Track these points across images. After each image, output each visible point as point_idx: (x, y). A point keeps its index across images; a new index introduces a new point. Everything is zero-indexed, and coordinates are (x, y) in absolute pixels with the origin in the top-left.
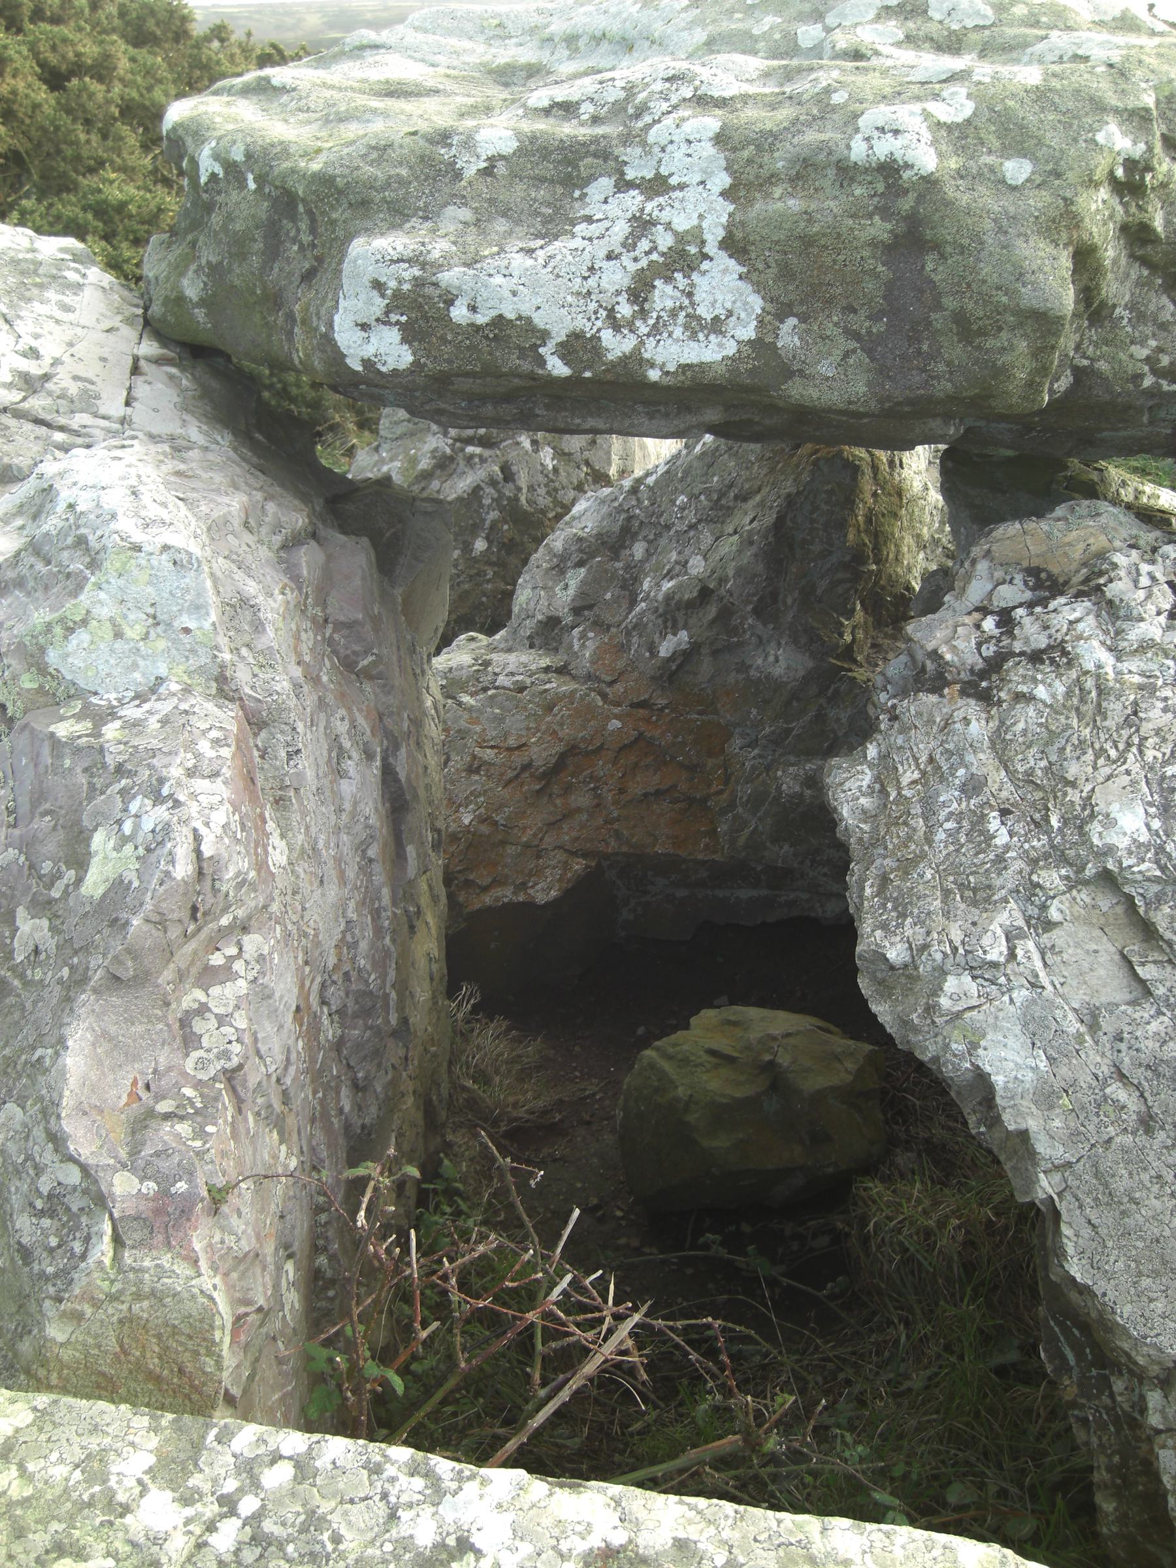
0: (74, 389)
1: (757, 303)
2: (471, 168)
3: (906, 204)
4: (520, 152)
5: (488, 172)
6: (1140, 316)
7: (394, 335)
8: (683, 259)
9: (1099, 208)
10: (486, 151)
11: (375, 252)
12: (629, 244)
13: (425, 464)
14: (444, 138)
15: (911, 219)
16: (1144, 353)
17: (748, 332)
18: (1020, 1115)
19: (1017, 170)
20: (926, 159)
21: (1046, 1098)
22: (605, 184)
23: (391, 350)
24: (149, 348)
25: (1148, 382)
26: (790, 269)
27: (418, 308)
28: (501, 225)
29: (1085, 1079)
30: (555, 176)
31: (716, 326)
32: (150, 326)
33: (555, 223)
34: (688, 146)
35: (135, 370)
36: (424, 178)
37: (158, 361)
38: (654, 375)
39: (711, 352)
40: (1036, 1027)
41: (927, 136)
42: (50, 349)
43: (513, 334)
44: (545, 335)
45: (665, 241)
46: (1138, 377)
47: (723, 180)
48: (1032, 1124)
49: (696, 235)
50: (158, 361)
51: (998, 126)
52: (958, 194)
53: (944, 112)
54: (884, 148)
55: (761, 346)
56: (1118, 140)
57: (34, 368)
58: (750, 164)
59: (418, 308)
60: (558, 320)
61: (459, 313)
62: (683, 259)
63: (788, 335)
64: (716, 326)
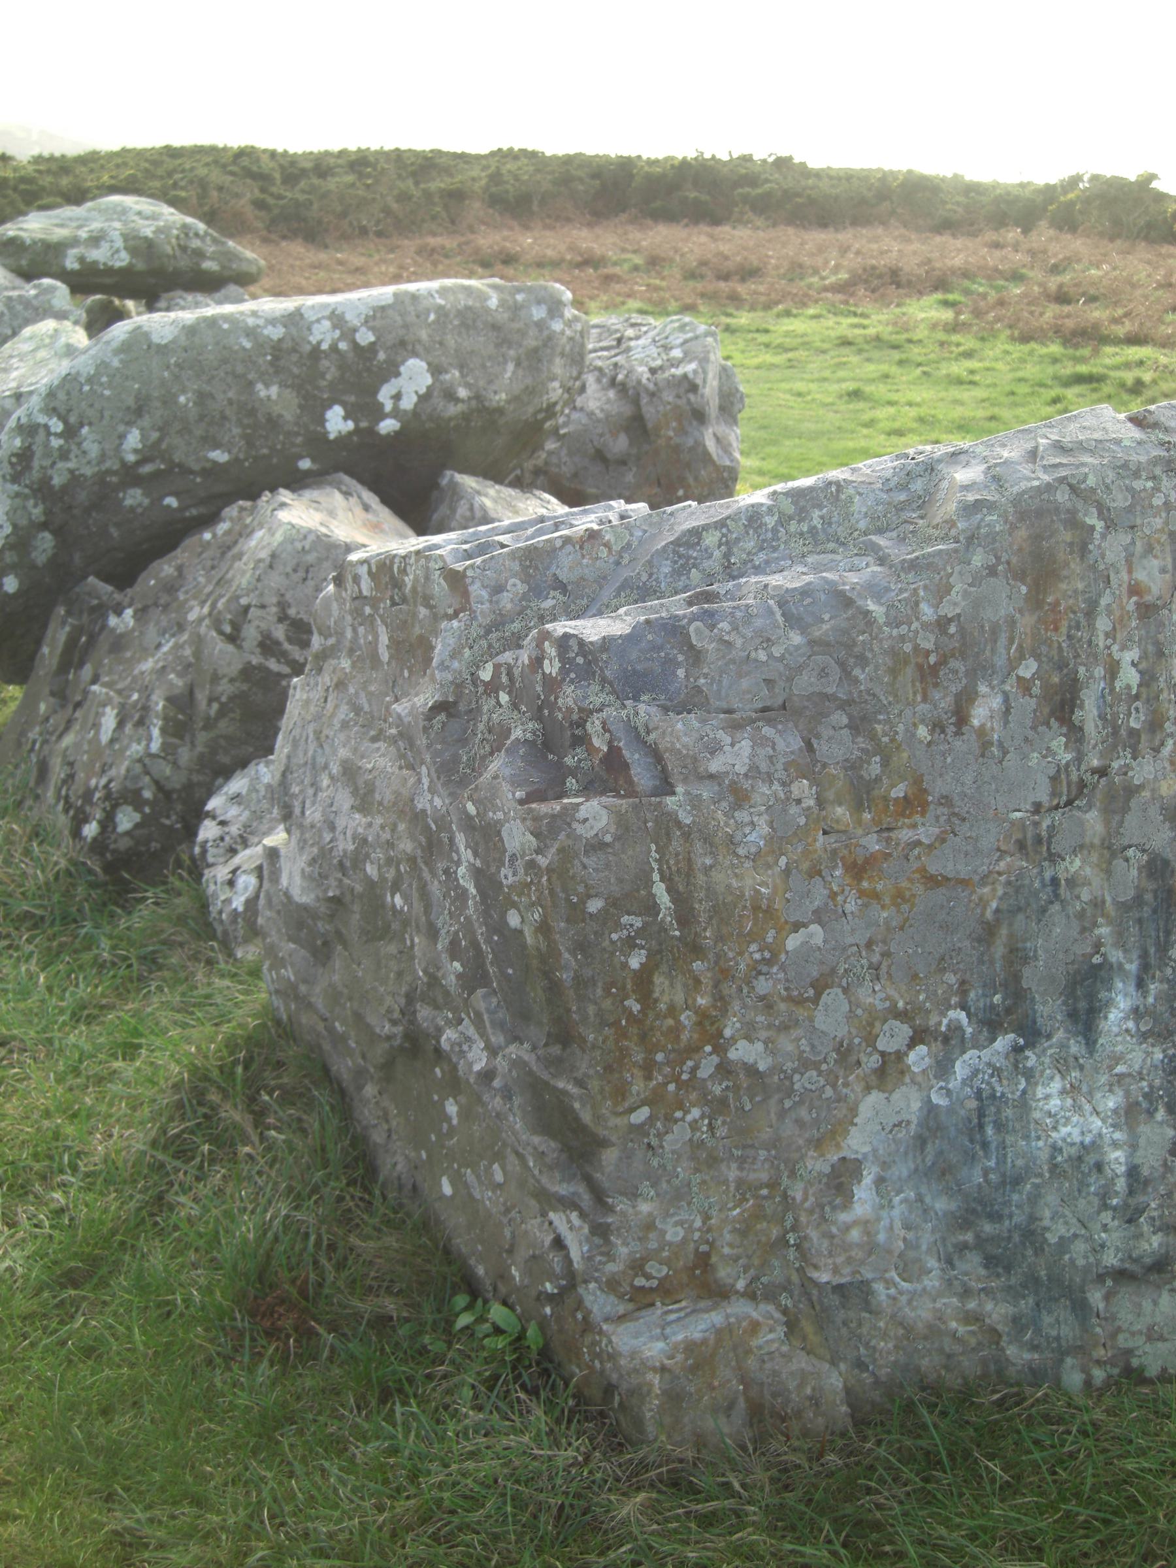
8: (117, 251)
9: (174, 241)
11: (73, 252)
15: (149, 244)
20: (151, 235)
23: (76, 266)
26: (133, 251)
27: (81, 260)
30: (95, 240)
34: (116, 235)
36: (75, 242)
39: (124, 264)
43: (95, 263)
51: (158, 231)
55: (130, 263)
56: (175, 232)
58: (126, 237)
59: (81, 260)
60: (102, 260)
62: (117, 251)
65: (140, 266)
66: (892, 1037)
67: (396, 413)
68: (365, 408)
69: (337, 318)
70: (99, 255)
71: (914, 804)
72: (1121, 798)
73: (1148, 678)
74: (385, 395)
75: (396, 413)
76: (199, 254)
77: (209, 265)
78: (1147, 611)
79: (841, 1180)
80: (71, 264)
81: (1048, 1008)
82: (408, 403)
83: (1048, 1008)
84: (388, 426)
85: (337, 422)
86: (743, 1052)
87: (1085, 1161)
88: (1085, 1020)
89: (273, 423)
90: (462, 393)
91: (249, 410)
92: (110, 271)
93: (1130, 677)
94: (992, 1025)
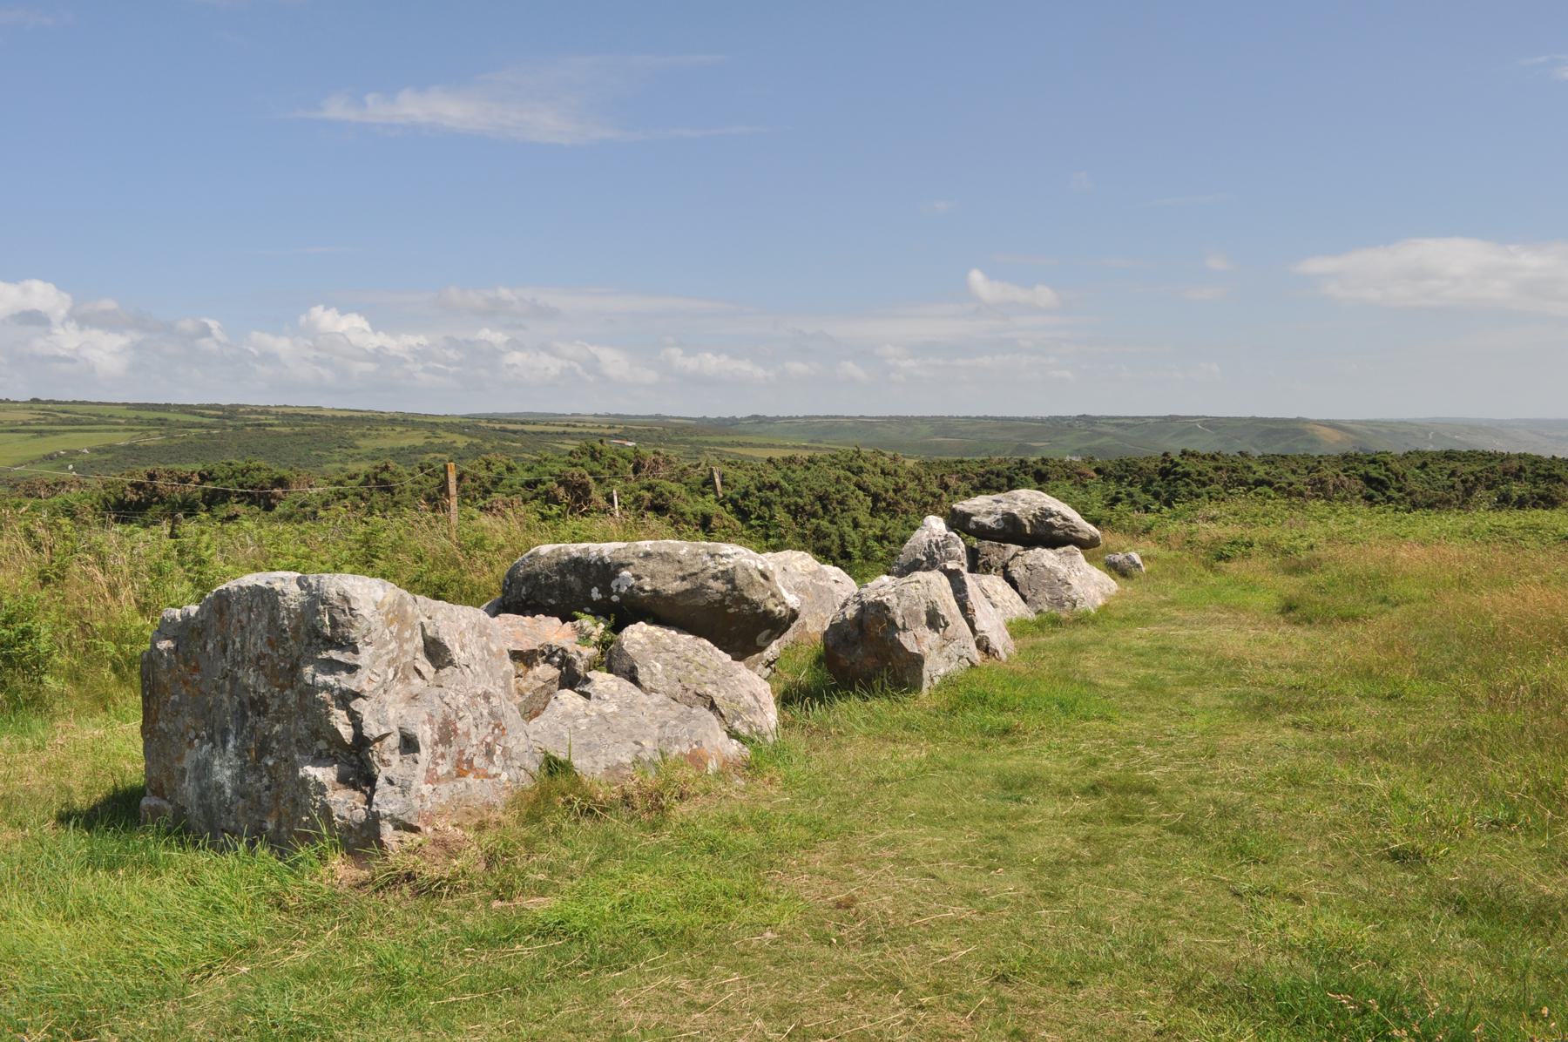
27: (977, 523)
65: (1010, 530)
66: (192, 734)
67: (618, 593)
68: (606, 590)
69: (601, 551)
70: (988, 521)
71: (196, 669)
72: (235, 680)
73: (243, 647)
74: (614, 584)
75: (618, 593)
76: (1051, 526)
77: (1055, 532)
78: (242, 628)
79: (183, 771)
80: (972, 526)
81: (218, 737)
82: (624, 589)
83: (218, 737)
84: (615, 598)
85: (596, 594)
86: (162, 725)
87: (220, 787)
88: (225, 743)
89: (571, 590)
90: (647, 588)
91: (562, 585)
92: (991, 530)
93: (238, 645)
94: (211, 738)
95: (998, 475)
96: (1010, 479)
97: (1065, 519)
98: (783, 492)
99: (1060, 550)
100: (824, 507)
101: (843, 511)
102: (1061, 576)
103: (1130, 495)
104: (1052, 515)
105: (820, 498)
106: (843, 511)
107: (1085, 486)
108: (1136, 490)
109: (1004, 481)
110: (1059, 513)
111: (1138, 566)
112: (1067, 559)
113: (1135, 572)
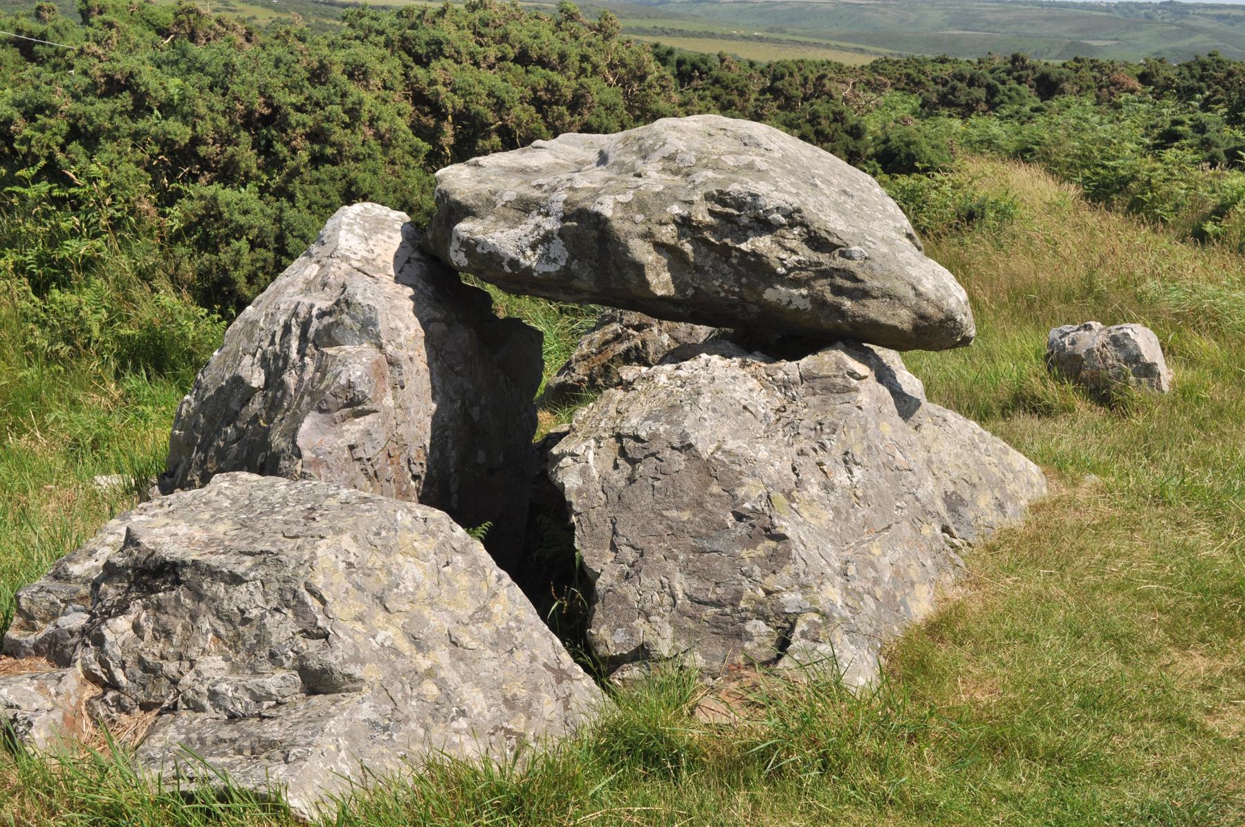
0: (381, 265)
1: (567, 254)
2: (500, 204)
3: (601, 227)
4: (516, 200)
5: (504, 206)
6: (716, 271)
7: (462, 254)
9: (668, 234)
10: (506, 198)
11: (464, 227)
12: (531, 233)
13: (610, 336)
14: (494, 193)
16: (717, 284)
17: (563, 263)
18: (571, 497)
19: (639, 218)
21: (579, 492)
22: (535, 212)
24: (416, 255)
25: (722, 294)
28: (502, 223)
29: (592, 489)
31: (555, 260)
32: (421, 249)
33: (515, 223)
35: (408, 262)
37: (418, 260)
38: (535, 274)
40: (584, 473)
41: (612, 206)
42: (377, 250)
44: (503, 259)
45: (542, 233)
46: (718, 293)
47: (561, 215)
48: (573, 500)
49: (551, 232)
50: (418, 260)
52: (616, 224)
53: (622, 198)
54: (598, 208)
55: (566, 268)
57: (370, 256)
61: (479, 249)
63: (575, 265)
64: (555, 260)
76: (758, 267)
77: (776, 294)
95: (972, 82)
96: (991, 90)
97: (817, 242)
98: (140, 107)
99: (789, 369)
100: (264, 148)
101: (317, 160)
102: (751, 493)
103: (1200, 128)
104: (764, 225)
105: (250, 121)
106: (317, 160)
107: (1117, 107)
108: (1214, 118)
109: (981, 93)
110: (794, 218)
111: (1148, 371)
112: (807, 411)
113: (1137, 390)
